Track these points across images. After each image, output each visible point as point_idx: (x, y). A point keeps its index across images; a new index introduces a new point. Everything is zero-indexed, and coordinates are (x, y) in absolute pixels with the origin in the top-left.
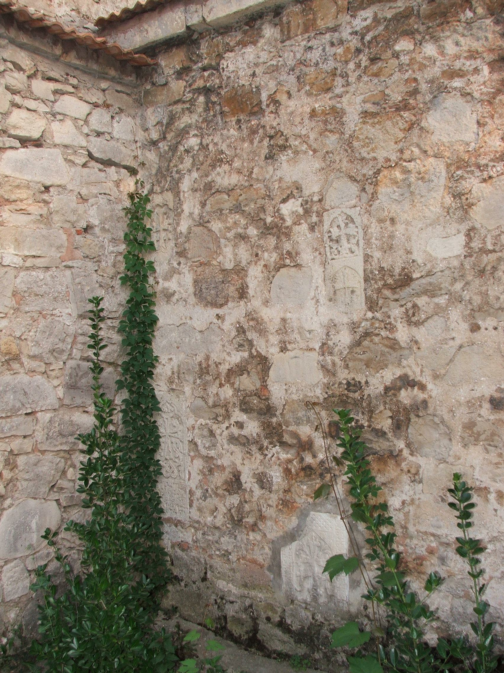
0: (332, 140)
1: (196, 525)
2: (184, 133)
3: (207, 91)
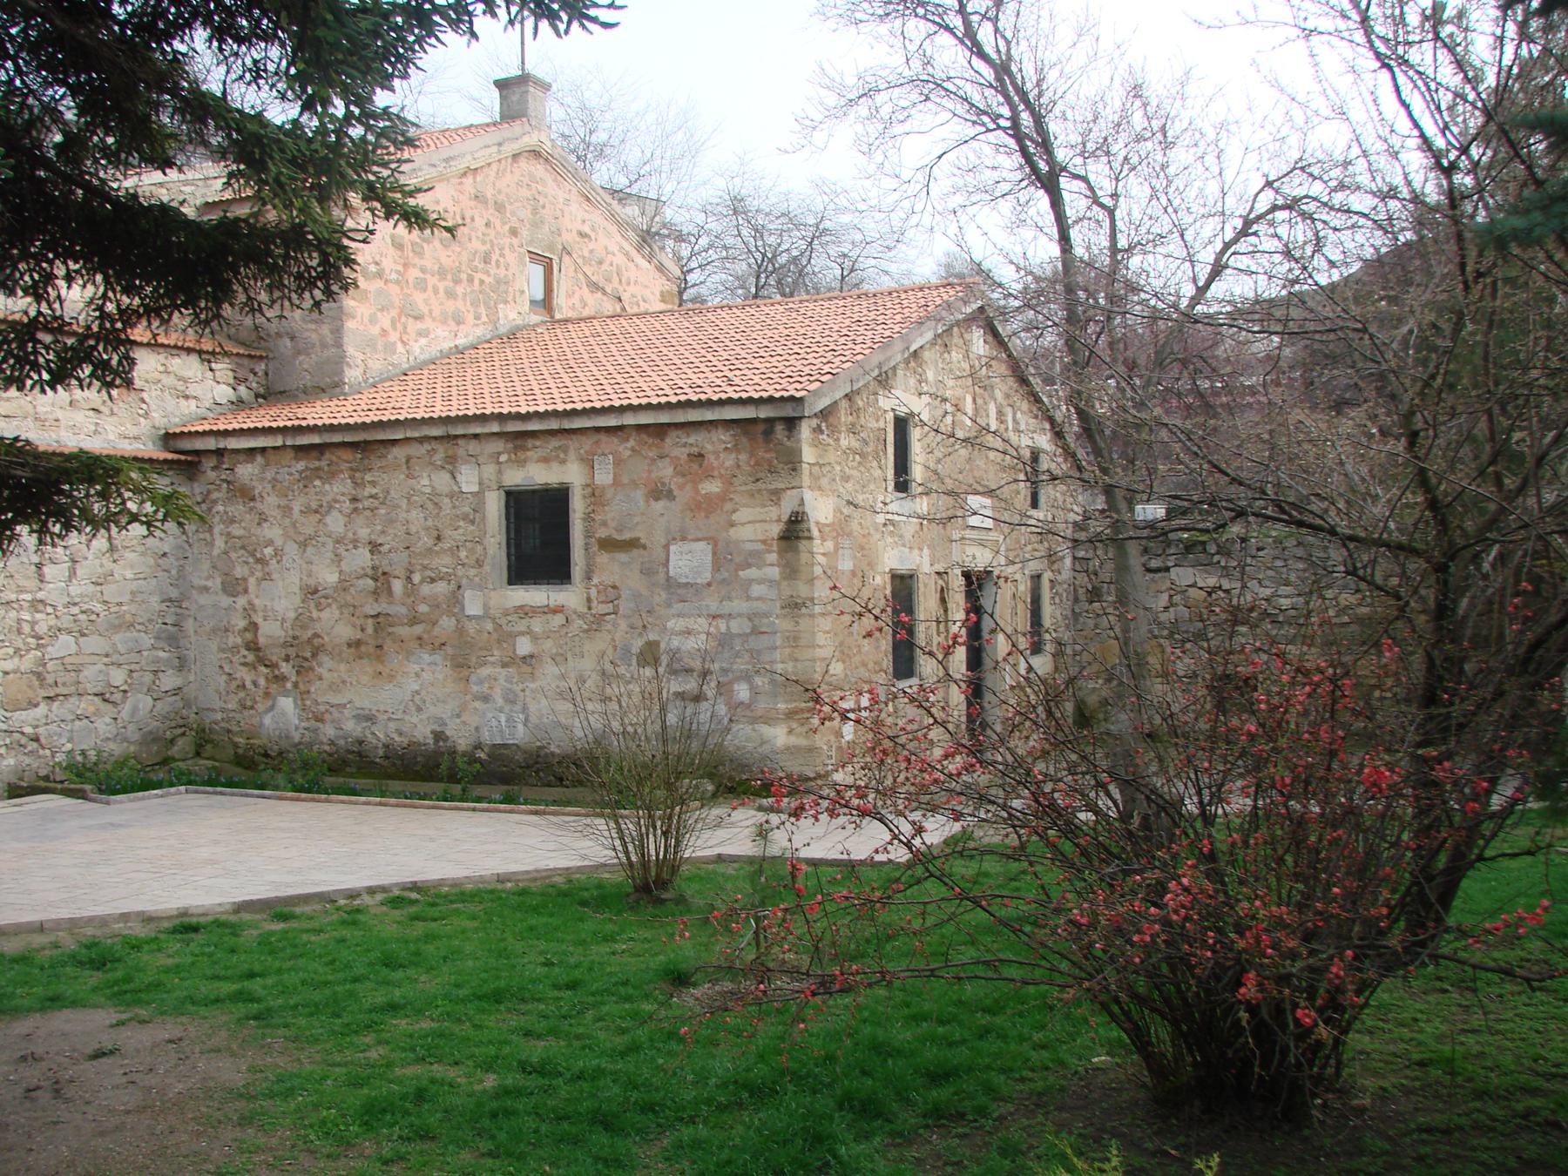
0: (287, 521)
1: (223, 710)
2: (215, 502)
3: (228, 482)
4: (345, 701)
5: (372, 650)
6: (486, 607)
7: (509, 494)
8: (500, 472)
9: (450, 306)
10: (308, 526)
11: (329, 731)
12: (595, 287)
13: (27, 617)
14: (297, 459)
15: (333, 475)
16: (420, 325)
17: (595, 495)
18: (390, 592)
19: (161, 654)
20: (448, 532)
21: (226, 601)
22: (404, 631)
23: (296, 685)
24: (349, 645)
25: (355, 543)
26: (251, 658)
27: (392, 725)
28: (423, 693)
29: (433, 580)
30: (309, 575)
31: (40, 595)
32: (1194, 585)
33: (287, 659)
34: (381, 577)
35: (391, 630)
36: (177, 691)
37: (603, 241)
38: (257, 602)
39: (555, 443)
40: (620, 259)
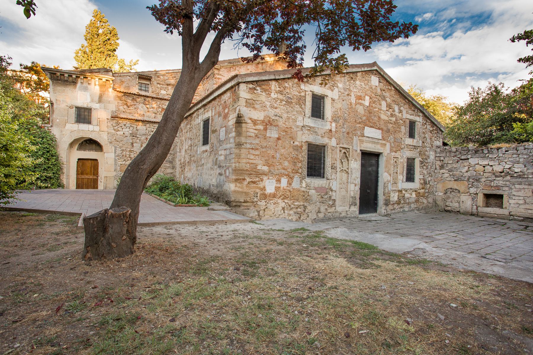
19: (167, 165)
31: (132, 149)
32: (478, 164)
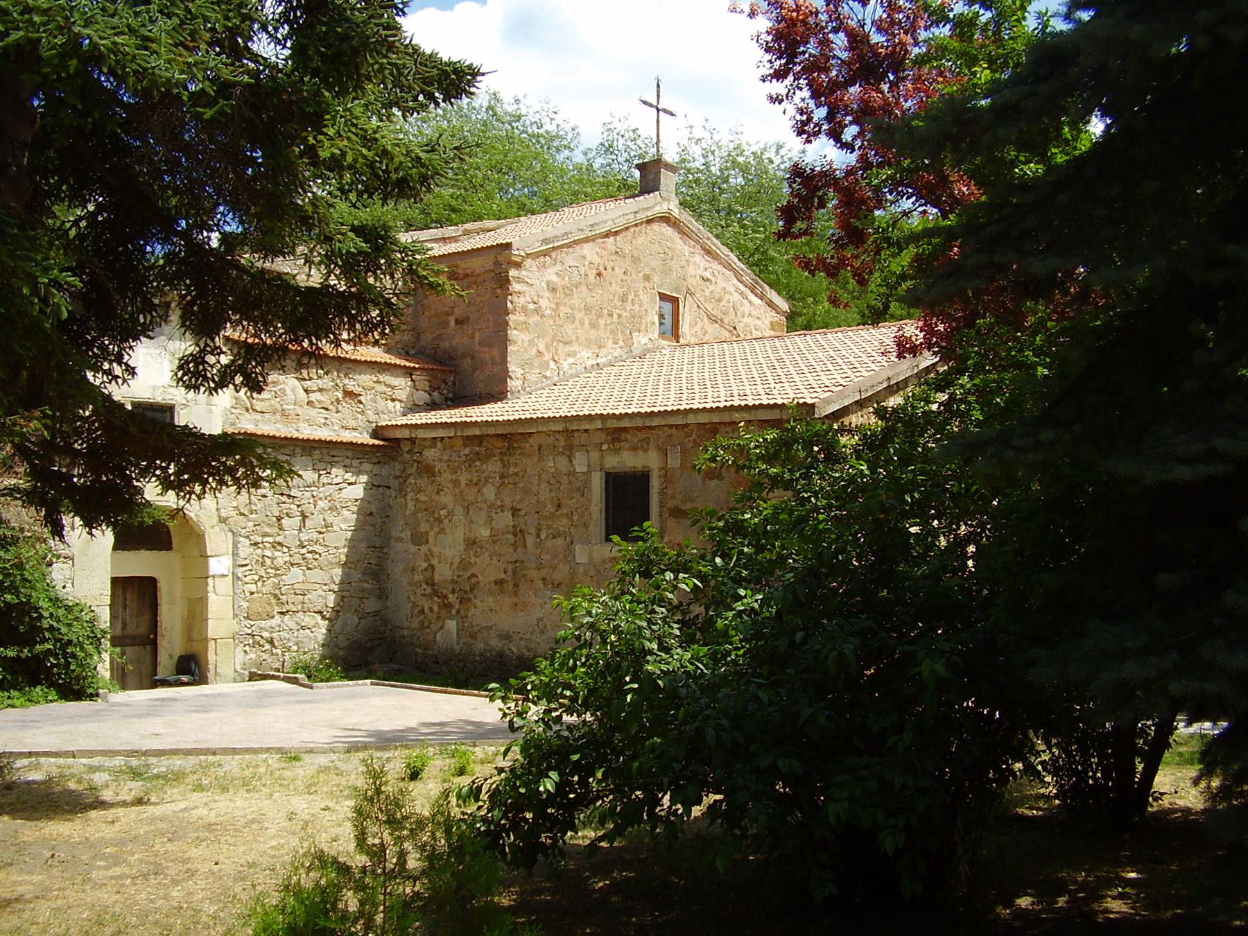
1: (408, 628)
4: (491, 624)
5: (510, 587)
6: (590, 557)
7: (608, 474)
8: (602, 457)
9: (593, 334)
10: (471, 494)
11: (480, 646)
12: (713, 319)
13: (269, 554)
14: (465, 446)
15: (488, 457)
16: (568, 348)
17: (666, 474)
18: (525, 545)
19: (366, 585)
20: (565, 501)
21: (414, 549)
22: (532, 573)
23: (458, 611)
24: (496, 583)
25: (502, 508)
26: (429, 590)
27: (522, 643)
28: (545, 620)
29: (554, 537)
30: (470, 531)
31: (279, 539)
33: (453, 592)
34: (518, 532)
35: (524, 572)
36: (377, 613)
37: (721, 284)
38: (434, 549)
39: (640, 436)
40: (736, 297)
